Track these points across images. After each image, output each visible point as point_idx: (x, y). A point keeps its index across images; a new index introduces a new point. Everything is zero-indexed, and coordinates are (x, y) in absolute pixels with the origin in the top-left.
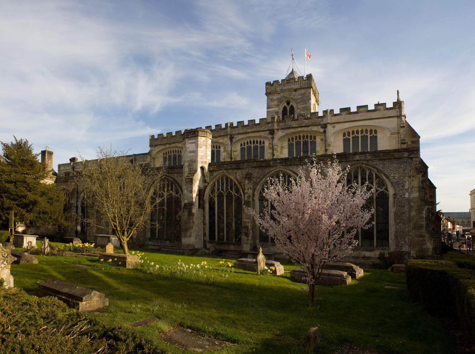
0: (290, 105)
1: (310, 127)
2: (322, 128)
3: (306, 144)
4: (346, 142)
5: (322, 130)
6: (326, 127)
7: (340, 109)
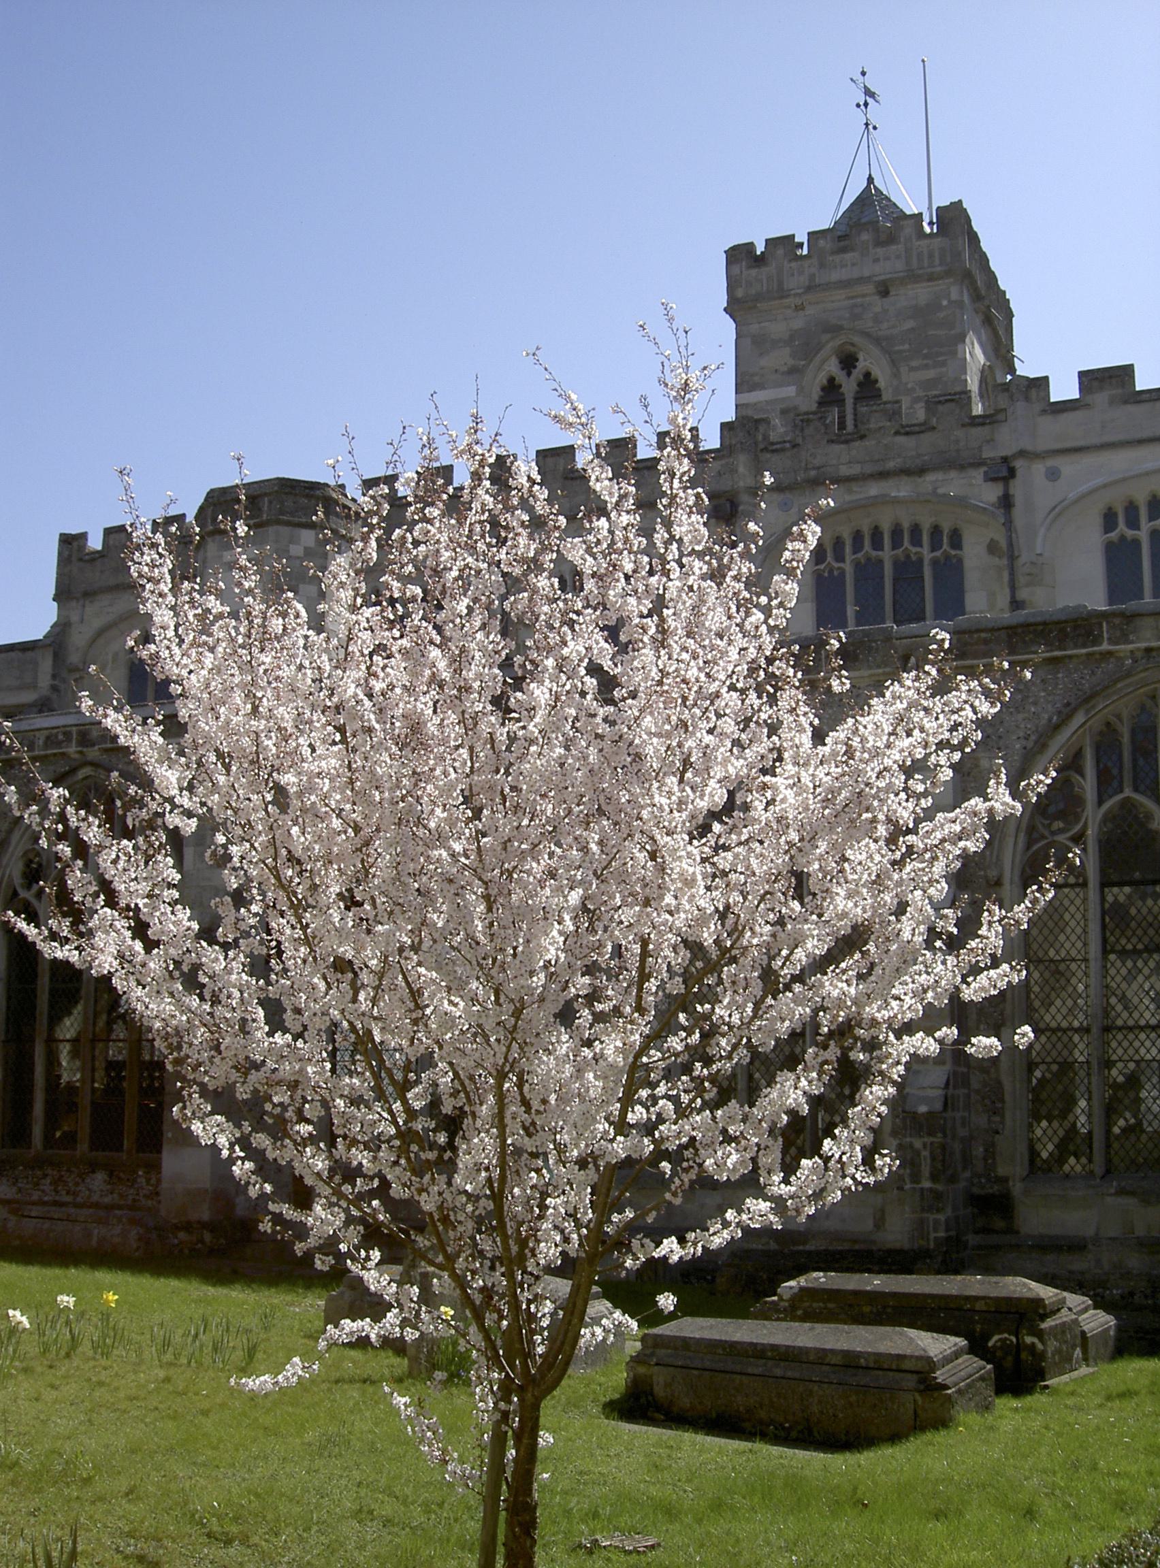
0: (857, 373)
1: (930, 477)
2: (990, 479)
3: (908, 571)
4: (1120, 558)
5: (991, 494)
6: (1012, 473)
7: (1082, 375)
